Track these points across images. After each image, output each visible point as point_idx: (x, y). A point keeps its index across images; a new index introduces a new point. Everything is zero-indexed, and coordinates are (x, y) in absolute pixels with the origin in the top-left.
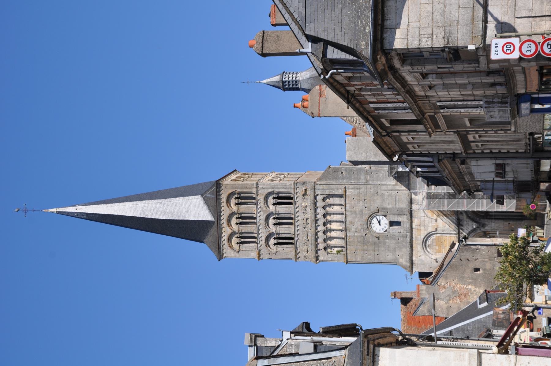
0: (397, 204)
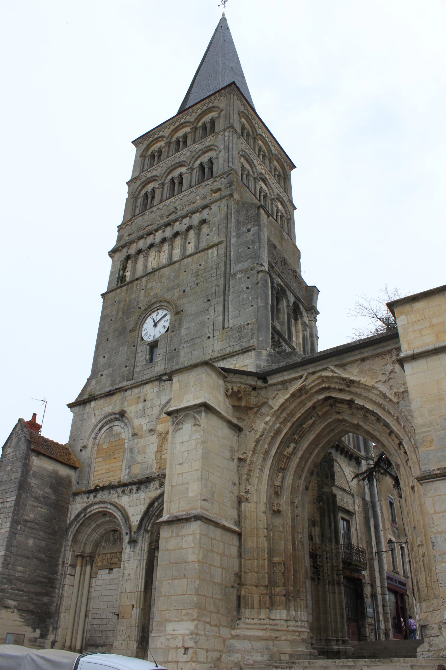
0: (185, 345)
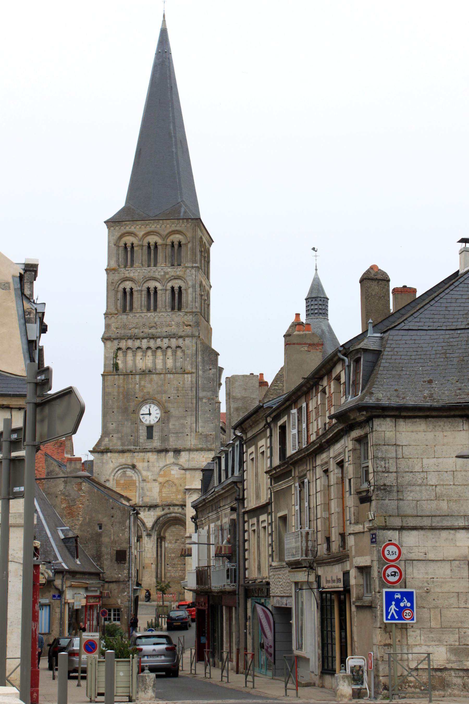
0: (172, 435)
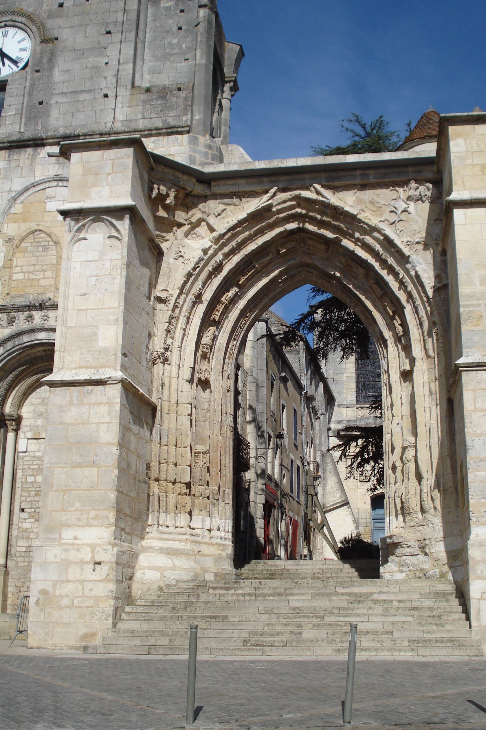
0: (60, 99)
